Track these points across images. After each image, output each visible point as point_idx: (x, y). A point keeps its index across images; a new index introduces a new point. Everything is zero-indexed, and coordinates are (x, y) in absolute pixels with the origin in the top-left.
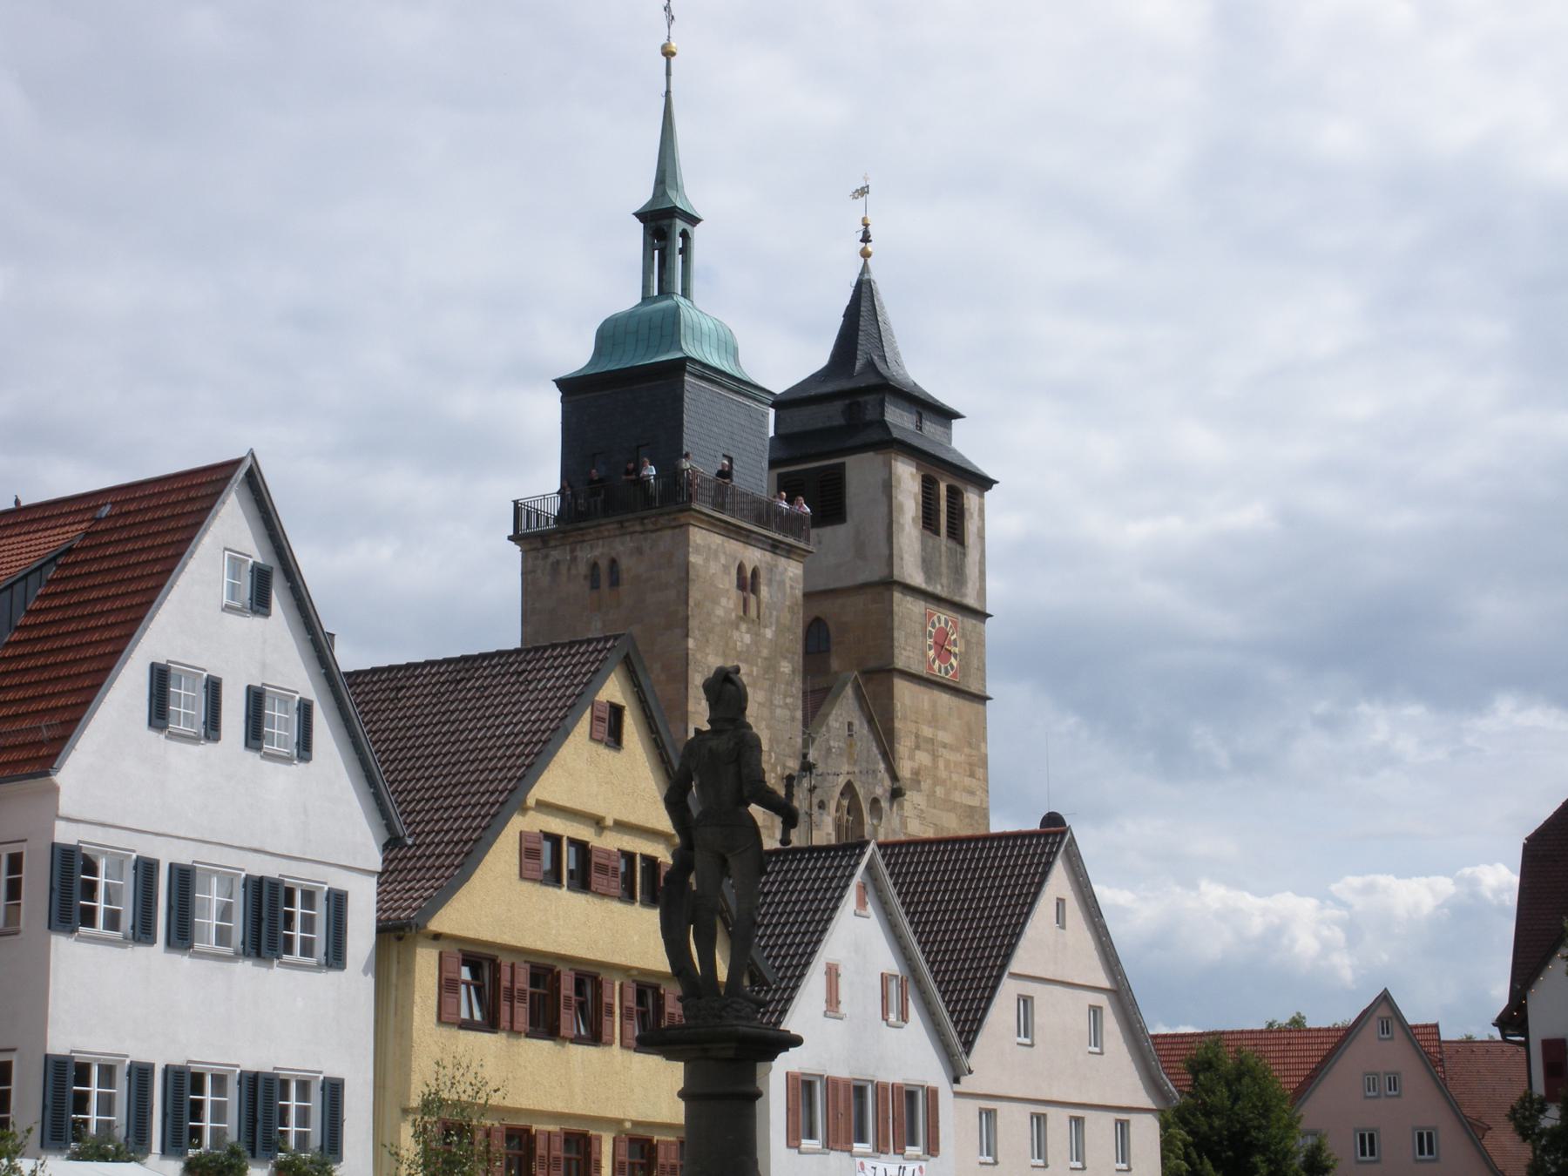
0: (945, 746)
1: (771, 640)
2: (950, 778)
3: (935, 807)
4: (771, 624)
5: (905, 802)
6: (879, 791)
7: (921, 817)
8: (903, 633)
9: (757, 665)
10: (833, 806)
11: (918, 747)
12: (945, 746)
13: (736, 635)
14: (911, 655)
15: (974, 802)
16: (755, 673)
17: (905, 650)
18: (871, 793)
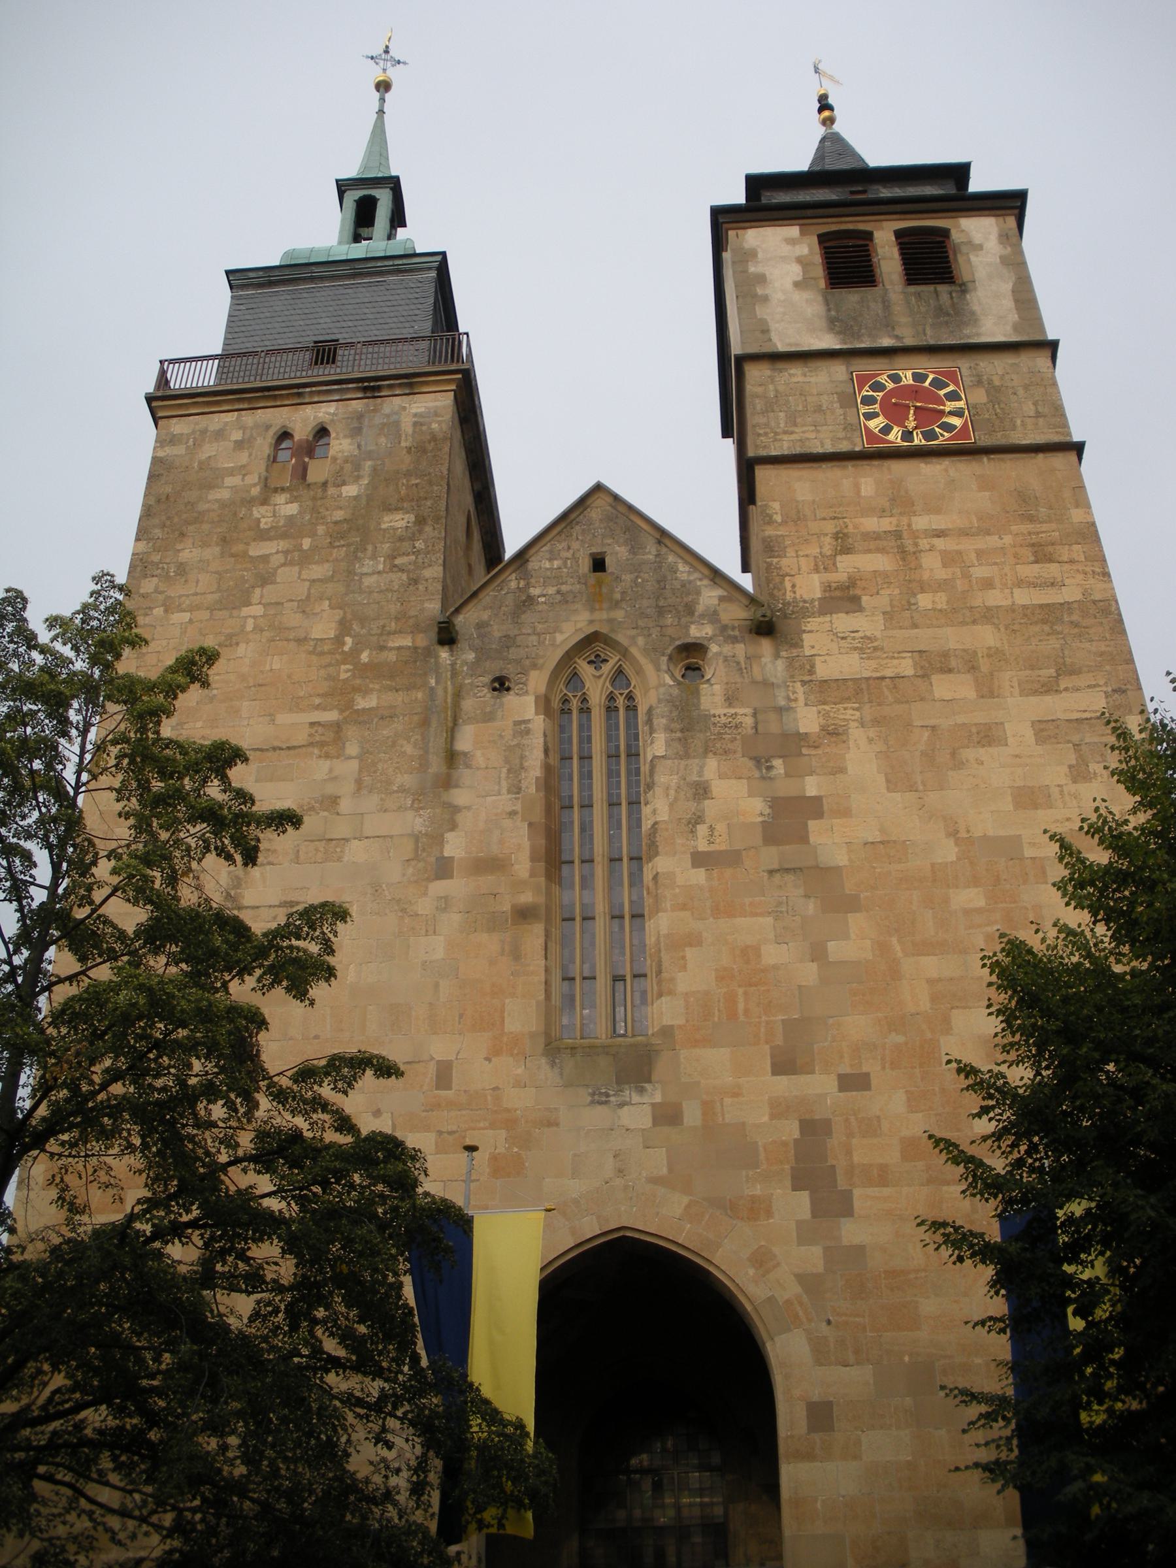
0: (940, 534)
1: (356, 498)
2: (966, 576)
3: (915, 626)
4: (358, 478)
5: (804, 636)
6: (696, 632)
7: (867, 647)
8: (782, 415)
9: (313, 534)
10: (538, 681)
11: (847, 550)
12: (940, 534)
13: (257, 511)
14: (812, 436)
15: (1070, 594)
16: (305, 547)
17: (792, 433)
18: (673, 639)
